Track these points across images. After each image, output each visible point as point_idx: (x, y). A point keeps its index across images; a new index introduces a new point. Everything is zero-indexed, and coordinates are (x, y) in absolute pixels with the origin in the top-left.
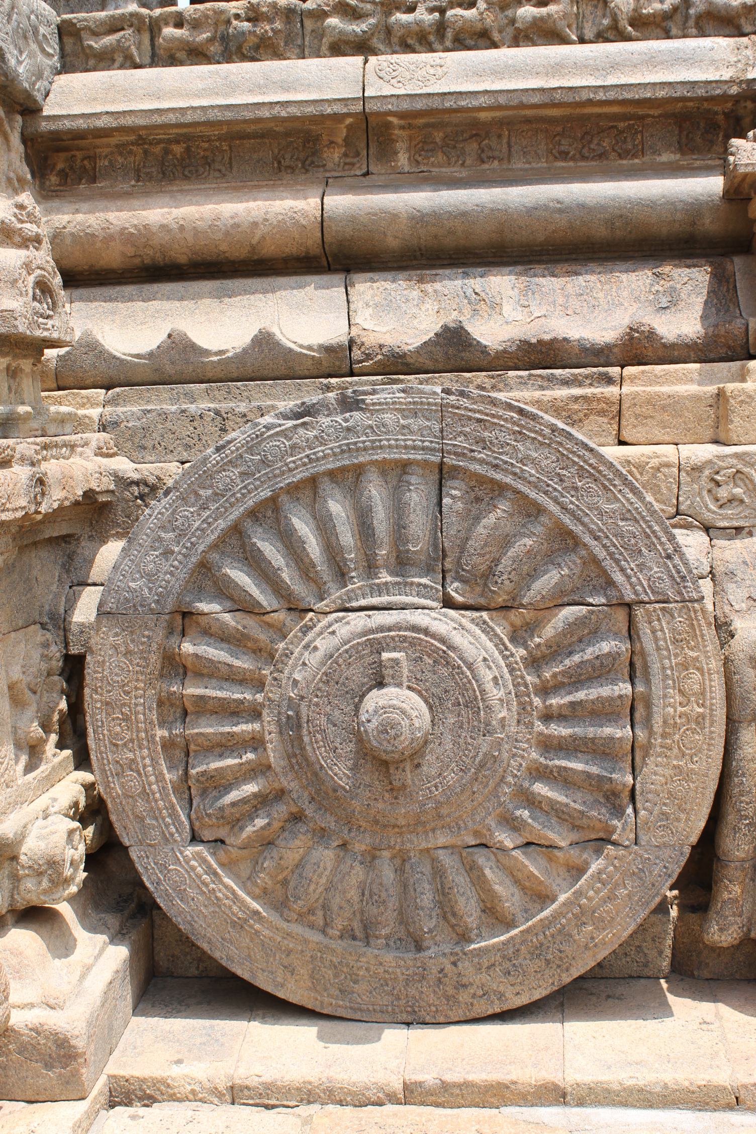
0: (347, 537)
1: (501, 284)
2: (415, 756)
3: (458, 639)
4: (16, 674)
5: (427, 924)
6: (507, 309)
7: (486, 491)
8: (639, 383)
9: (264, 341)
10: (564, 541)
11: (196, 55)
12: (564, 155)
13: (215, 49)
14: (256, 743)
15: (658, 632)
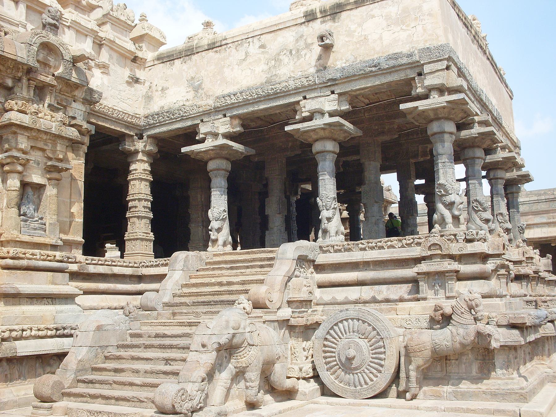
0: (347, 329)
1: (384, 287)
2: (353, 358)
3: (360, 343)
4: (304, 346)
5: (357, 384)
6: (385, 293)
7: (364, 322)
8: (401, 305)
9: (346, 298)
10: (374, 329)
11: (340, 251)
12: (397, 266)
13: (343, 250)
14: (335, 357)
15: (387, 342)
